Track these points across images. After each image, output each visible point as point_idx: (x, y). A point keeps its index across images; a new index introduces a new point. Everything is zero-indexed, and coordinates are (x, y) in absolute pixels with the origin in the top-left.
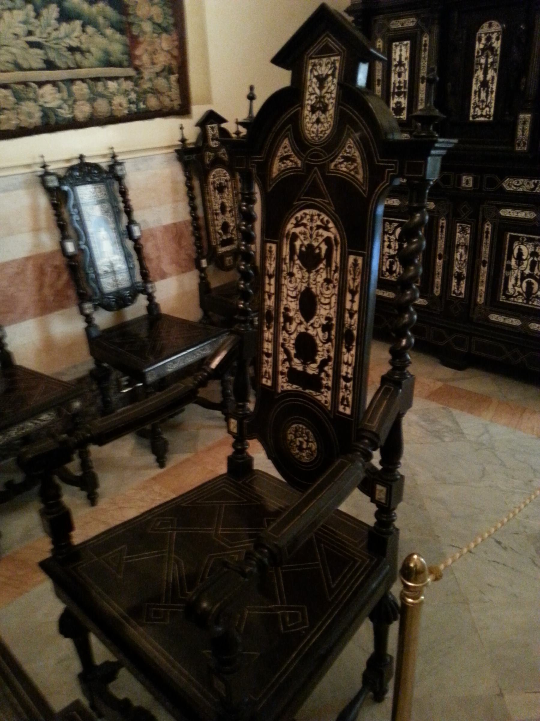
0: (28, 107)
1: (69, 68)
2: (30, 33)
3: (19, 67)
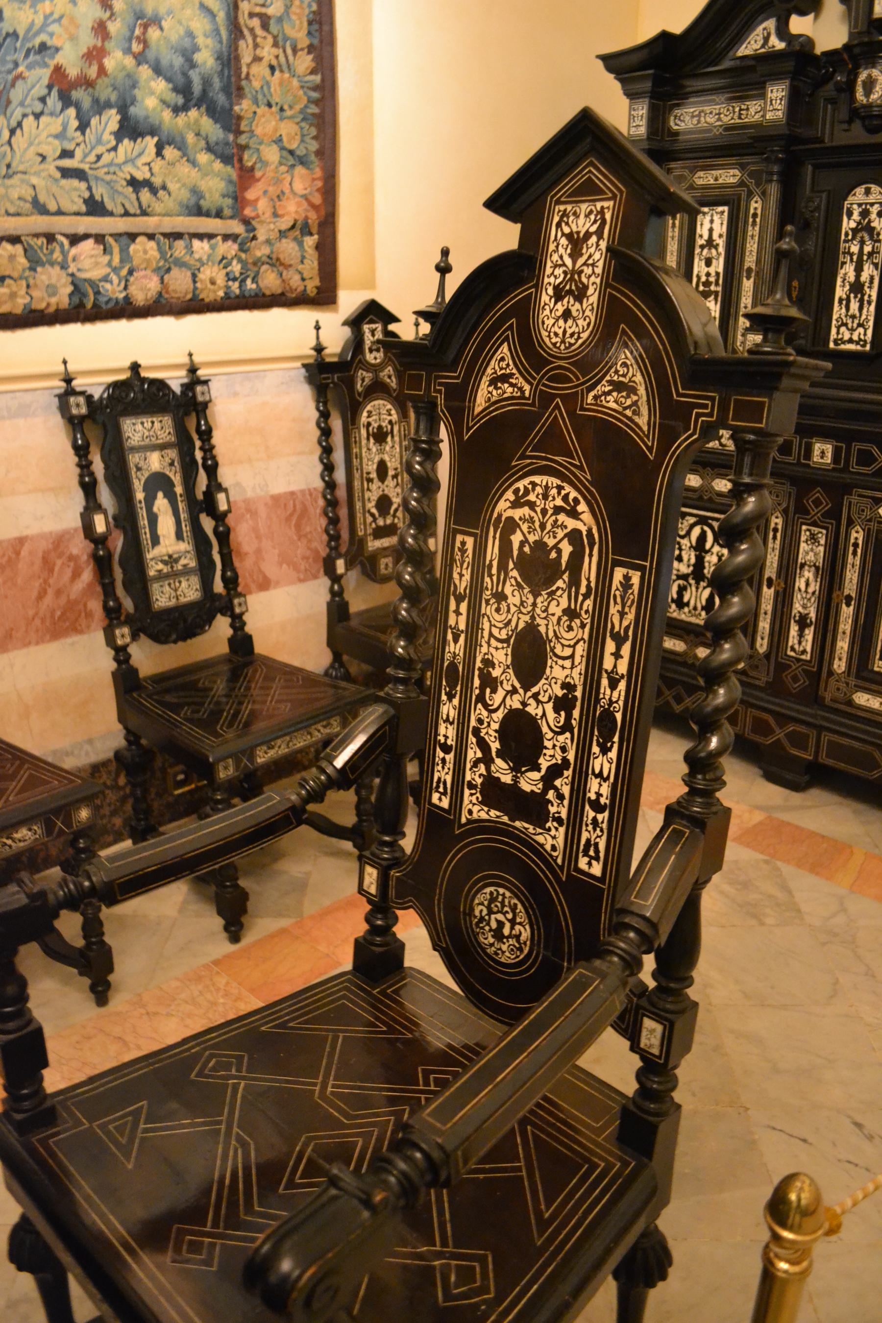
1: (126, 214)
2: (66, 154)
3: (40, 209)
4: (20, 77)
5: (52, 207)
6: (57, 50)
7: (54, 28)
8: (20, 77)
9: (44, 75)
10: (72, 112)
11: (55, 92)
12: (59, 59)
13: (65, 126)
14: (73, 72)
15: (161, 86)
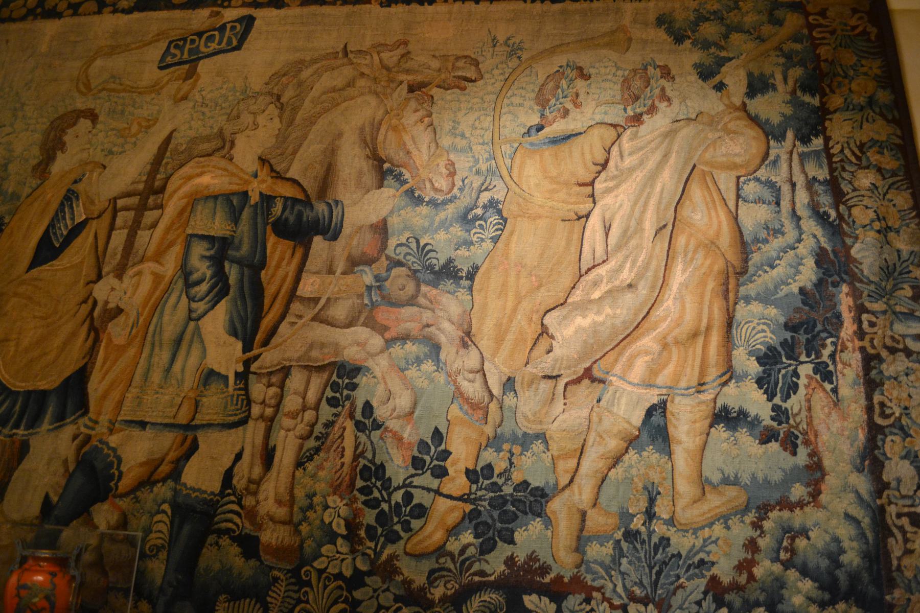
4: (681, 586)
6: (713, 563)
7: (712, 547)
8: (681, 586)
9: (702, 583)
11: (710, 597)
12: (715, 570)
14: (726, 580)
15: (807, 585)
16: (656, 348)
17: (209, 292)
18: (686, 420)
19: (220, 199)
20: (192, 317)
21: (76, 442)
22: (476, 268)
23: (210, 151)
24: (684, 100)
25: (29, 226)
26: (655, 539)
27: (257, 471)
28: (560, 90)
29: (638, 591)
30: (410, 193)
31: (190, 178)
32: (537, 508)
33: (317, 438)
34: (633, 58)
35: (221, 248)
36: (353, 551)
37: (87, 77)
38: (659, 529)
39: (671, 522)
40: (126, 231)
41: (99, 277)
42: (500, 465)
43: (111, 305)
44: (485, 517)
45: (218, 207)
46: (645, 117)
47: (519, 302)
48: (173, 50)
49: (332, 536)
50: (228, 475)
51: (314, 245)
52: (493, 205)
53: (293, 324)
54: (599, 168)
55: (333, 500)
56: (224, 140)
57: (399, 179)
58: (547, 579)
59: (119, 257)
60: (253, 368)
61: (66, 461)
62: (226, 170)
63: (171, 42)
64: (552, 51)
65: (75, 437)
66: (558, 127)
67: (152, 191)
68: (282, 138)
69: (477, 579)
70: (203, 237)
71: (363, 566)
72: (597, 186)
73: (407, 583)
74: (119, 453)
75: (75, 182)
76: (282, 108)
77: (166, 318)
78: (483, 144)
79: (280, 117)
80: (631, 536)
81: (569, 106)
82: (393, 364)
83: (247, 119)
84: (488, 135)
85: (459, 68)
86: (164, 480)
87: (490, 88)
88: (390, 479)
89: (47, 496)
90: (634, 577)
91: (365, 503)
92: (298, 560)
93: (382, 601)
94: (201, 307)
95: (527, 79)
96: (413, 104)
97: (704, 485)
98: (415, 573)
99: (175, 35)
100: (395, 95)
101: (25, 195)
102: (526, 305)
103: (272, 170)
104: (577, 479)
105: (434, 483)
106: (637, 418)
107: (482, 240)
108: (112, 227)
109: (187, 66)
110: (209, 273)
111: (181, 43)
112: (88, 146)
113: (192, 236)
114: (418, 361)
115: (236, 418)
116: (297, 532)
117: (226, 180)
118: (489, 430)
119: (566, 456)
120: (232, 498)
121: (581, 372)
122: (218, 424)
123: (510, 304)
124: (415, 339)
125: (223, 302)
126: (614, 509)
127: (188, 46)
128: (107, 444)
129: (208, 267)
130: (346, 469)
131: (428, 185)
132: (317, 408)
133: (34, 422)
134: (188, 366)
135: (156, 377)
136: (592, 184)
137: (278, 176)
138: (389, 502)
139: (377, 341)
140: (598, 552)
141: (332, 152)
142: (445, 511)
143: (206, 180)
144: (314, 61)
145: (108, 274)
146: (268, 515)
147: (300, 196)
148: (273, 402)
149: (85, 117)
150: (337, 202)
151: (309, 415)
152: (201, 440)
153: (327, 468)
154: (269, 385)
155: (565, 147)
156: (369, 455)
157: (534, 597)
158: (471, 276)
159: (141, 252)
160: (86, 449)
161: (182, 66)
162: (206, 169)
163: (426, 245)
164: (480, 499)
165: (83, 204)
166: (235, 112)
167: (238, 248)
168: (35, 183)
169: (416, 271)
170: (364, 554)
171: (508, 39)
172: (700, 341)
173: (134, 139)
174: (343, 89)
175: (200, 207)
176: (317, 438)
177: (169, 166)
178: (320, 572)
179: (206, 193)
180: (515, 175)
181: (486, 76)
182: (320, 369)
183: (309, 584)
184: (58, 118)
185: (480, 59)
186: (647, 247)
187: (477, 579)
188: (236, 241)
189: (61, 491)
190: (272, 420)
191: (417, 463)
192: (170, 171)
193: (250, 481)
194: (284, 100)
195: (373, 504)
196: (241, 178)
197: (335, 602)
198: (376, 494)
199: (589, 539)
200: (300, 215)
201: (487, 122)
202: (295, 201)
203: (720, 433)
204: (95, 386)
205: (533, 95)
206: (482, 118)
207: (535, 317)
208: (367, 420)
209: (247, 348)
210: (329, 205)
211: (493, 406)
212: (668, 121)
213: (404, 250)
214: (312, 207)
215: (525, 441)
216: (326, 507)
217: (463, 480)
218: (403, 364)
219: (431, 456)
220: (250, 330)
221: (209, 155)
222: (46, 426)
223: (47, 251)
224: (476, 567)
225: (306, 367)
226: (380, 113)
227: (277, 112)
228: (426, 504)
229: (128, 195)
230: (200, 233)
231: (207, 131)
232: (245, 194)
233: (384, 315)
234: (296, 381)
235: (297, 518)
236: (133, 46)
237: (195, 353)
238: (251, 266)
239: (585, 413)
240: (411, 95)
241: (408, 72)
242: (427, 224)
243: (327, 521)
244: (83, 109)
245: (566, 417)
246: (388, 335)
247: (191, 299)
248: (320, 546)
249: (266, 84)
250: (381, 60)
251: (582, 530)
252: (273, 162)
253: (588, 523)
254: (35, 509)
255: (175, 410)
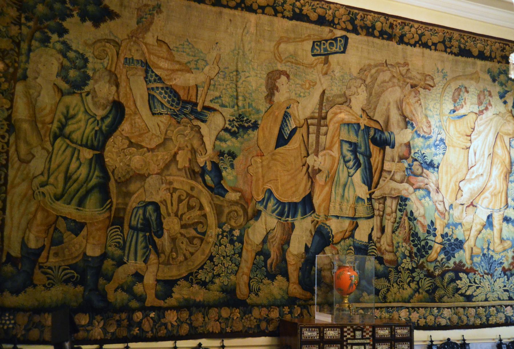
0: (501, 315)
2: (505, 286)
3: (499, 299)
5: (502, 299)
9: (501, 269)
10: (506, 276)
12: (504, 265)
13: (504, 280)
16: (490, 196)
17: (354, 165)
18: (497, 220)
19: (350, 125)
20: (350, 176)
21: (313, 223)
22: (439, 164)
23: (342, 102)
24: (496, 105)
25: (270, 127)
26: (490, 256)
27: (379, 234)
28: (460, 97)
29: (486, 271)
30: (416, 132)
31: (336, 114)
32: (461, 246)
33: (398, 223)
34: (481, 85)
35: (354, 147)
36: (411, 261)
37: (278, 52)
38: (491, 253)
39: (493, 251)
40: (315, 135)
41: (308, 155)
42: (450, 233)
43: (316, 168)
44: (447, 249)
45: (350, 130)
46: (484, 111)
47: (452, 178)
48: (316, 47)
49: (405, 256)
50: (370, 236)
51: (386, 150)
52: (442, 140)
53: (384, 180)
54: (472, 130)
55: (404, 244)
56: (347, 98)
57: (412, 125)
58: (465, 268)
59: (314, 146)
60: (373, 196)
61: (311, 231)
62: (349, 112)
63: (314, 42)
64: (456, 78)
65: (312, 222)
66: (461, 112)
67: (321, 119)
68: (369, 100)
69: (447, 268)
70: (346, 142)
71: (415, 266)
72: (472, 136)
73: (428, 270)
74: (331, 228)
75: (287, 108)
76: (366, 86)
77: (341, 175)
78: (437, 115)
79: (366, 91)
80: (484, 255)
81: (463, 103)
82: (417, 198)
83: (354, 89)
84: (438, 111)
85: (428, 80)
86: (348, 238)
87: (438, 91)
88: (420, 237)
89: (306, 245)
90: (485, 267)
91: (413, 245)
92: (396, 264)
93: (421, 276)
94: (352, 171)
95: (449, 89)
96: (413, 94)
97: (502, 240)
98: (431, 267)
99: (317, 38)
100: (406, 88)
101: (264, 111)
102: (454, 179)
103: (368, 115)
104: (470, 238)
105: (433, 239)
106: (485, 219)
107: (440, 154)
108: (308, 133)
109: (323, 57)
110: (352, 157)
111: (319, 44)
112: (288, 90)
113: (343, 140)
114: (424, 197)
115: (370, 215)
116: (396, 255)
117: (351, 117)
118: (446, 221)
119: (467, 230)
120: (373, 244)
121: (470, 203)
122: (364, 218)
123: (449, 179)
124: (423, 189)
125: (359, 170)
126: (480, 247)
127: (322, 46)
128: (326, 224)
129: (351, 155)
130: (406, 234)
131: (421, 130)
132: (396, 212)
133: (294, 216)
134: (350, 195)
135: (339, 199)
136: (470, 136)
137: (370, 118)
138: (420, 245)
139: (411, 189)
140: (477, 260)
141: (388, 110)
142: (437, 247)
143: (342, 116)
144: (376, 66)
145: (312, 153)
146: (385, 249)
147: (380, 129)
148: (382, 210)
149: (283, 74)
150: (392, 133)
151: (394, 214)
152: (359, 223)
153: (402, 233)
154: (380, 204)
155: (461, 120)
156: (414, 229)
157: (462, 273)
158: (438, 167)
159: (323, 145)
160: (317, 226)
161: (321, 57)
162: (343, 111)
163: (424, 153)
164: (445, 244)
165: (294, 120)
166: (349, 86)
167: (361, 148)
168: (268, 106)
169: (421, 163)
170: (414, 262)
171: (443, 70)
172: (500, 194)
173: (308, 91)
174: (388, 82)
175: (342, 128)
176: (398, 223)
177: (327, 107)
178: (403, 268)
179: (344, 122)
180: (447, 129)
181: (437, 85)
182: (395, 198)
183: (401, 272)
184: (270, 73)
185: (434, 77)
186: (487, 162)
187: (447, 268)
188: (359, 145)
189: (311, 243)
190: (382, 216)
191: (428, 232)
192: (327, 110)
193: (377, 238)
194: (367, 83)
195: (415, 245)
196: (356, 117)
197: (408, 277)
198: (416, 242)
199: (475, 256)
200: (380, 137)
201: (438, 106)
202: (379, 130)
203: (505, 224)
204: (317, 201)
205: (451, 97)
206: (437, 104)
207: (457, 184)
208: (412, 218)
209: (370, 189)
210: (389, 133)
211: (447, 214)
212: (492, 114)
213: (418, 155)
214: (384, 134)
215: (456, 225)
216: (403, 247)
217: (440, 237)
218: (420, 198)
219: (431, 229)
220: (369, 181)
221: (342, 104)
222: (299, 217)
223: (282, 140)
224: (446, 265)
225: (391, 197)
226: (402, 96)
227: (365, 88)
228: (432, 245)
229: (312, 118)
230: (345, 139)
231: (339, 93)
232: (359, 125)
233: (413, 179)
234: (388, 202)
235: (395, 251)
236: (298, 40)
237: (351, 190)
238: (367, 156)
239: (472, 217)
240: (412, 89)
241: (410, 78)
242: (423, 145)
243: (403, 251)
244: (281, 70)
245: (467, 218)
246: (415, 187)
247: (348, 168)
248: (402, 259)
249: (359, 73)
250: (400, 71)
251: (472, 253)
252: (367, 111)
253: (474, 251)
254: (303, 250)
255: (348, 211)
